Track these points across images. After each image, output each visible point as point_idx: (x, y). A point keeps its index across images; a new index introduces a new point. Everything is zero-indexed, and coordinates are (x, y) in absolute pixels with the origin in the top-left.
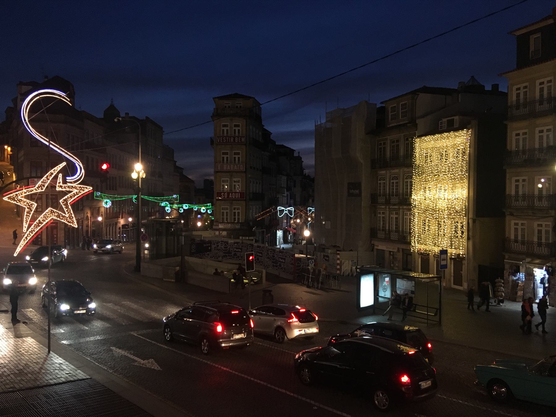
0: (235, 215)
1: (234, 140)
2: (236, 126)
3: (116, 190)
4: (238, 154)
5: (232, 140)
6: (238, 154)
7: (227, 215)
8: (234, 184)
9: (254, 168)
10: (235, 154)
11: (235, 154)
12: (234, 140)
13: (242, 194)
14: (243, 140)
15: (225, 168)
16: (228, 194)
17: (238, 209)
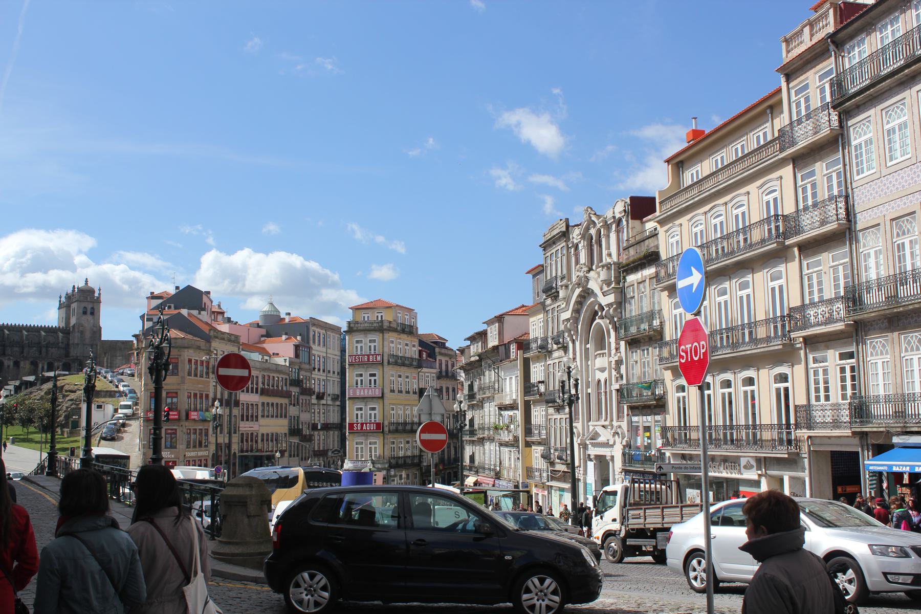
0: (371, 451)
1: (368, 359)
2: (370, 341)
3: (257, 420)
4: (374, 375)
5: (366, 359)
6: (374, 375)
7: (362, 451)
8: (369, 412)
9: (400, 392)
10: (371, 375)
11: (371, 375)
12: (368, 359)
13: (378, 425)
14: (379, 358)
15: (358, 394)
16: (362, 424)
17: (375, 443)
